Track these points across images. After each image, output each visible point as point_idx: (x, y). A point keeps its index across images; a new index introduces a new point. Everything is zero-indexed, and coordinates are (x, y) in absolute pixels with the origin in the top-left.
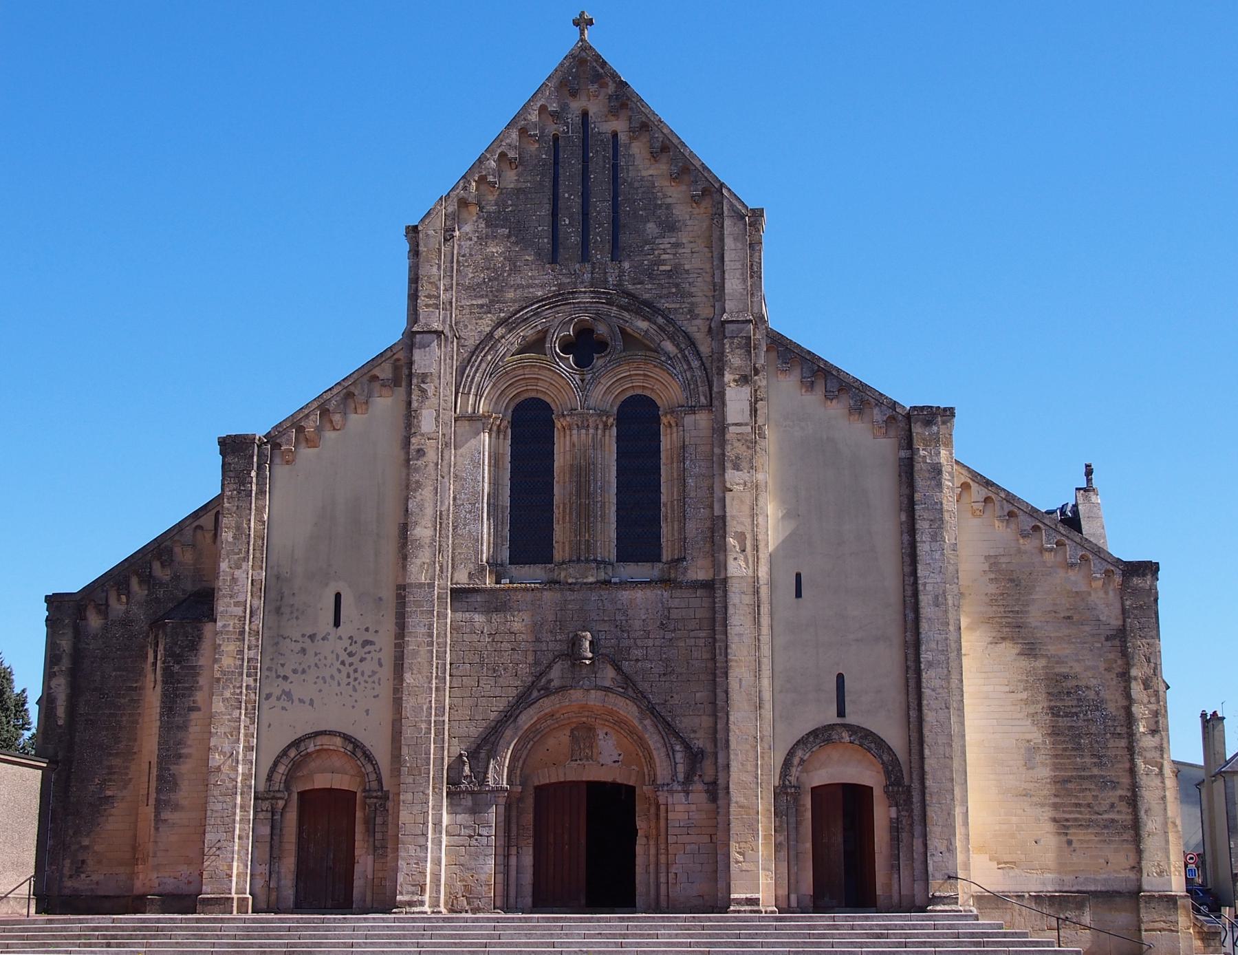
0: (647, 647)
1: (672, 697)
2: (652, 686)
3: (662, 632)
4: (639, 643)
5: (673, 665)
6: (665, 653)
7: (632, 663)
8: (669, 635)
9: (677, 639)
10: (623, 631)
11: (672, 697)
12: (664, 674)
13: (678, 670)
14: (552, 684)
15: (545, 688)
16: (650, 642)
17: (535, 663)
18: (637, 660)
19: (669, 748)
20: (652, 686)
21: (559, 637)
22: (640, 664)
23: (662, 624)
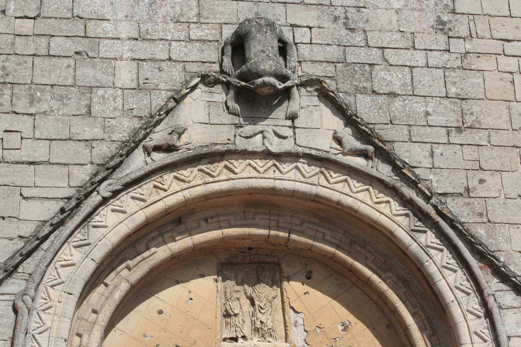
0: (411, 67)
1: (481, 181)
2: (432, 155)
3: (442, 39)
4: (392, 56)
5: (476, 109)
6: (454, 83)
7: (381, 99)
8: (458, 46)
9: (479, 54)
10: (352, 30)
11: (481, 181)
12: (459, 129)
13: (488, 121)
14: (184, 138)
15: (170, 149)
16: (419, 59)
17: (138, 88)
18: (393, 95)
19: (491, 300)
20: (432, 155)
21: (196, 33)
22: (398, 103)
23: (440, 21)
